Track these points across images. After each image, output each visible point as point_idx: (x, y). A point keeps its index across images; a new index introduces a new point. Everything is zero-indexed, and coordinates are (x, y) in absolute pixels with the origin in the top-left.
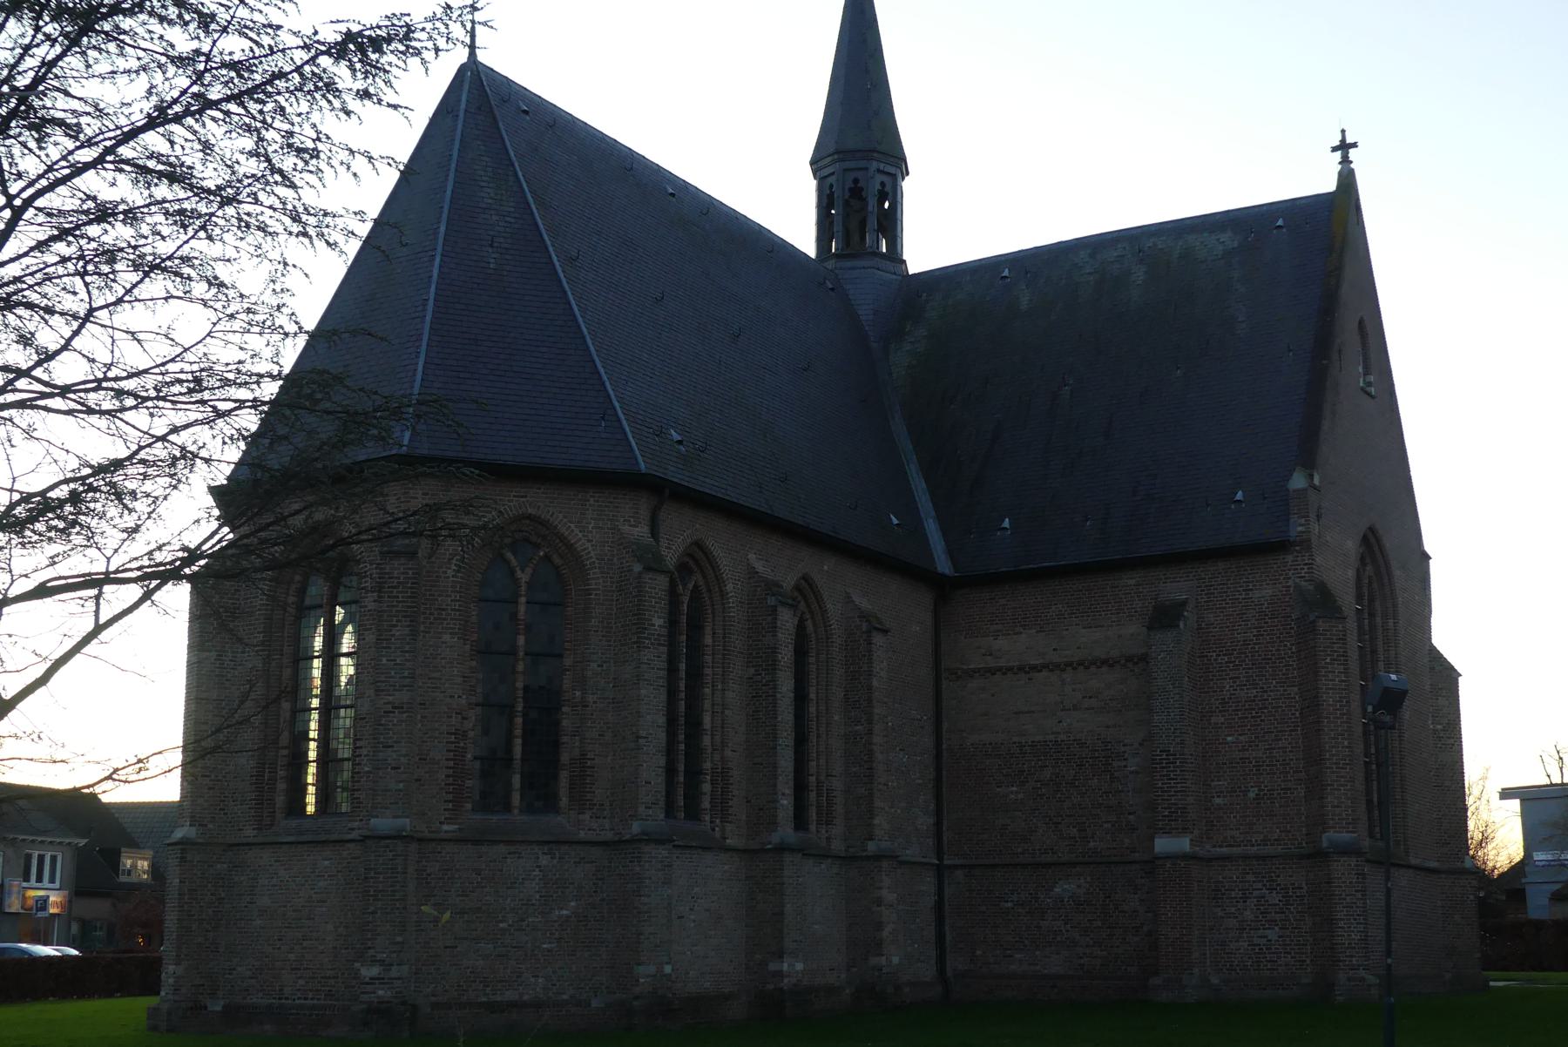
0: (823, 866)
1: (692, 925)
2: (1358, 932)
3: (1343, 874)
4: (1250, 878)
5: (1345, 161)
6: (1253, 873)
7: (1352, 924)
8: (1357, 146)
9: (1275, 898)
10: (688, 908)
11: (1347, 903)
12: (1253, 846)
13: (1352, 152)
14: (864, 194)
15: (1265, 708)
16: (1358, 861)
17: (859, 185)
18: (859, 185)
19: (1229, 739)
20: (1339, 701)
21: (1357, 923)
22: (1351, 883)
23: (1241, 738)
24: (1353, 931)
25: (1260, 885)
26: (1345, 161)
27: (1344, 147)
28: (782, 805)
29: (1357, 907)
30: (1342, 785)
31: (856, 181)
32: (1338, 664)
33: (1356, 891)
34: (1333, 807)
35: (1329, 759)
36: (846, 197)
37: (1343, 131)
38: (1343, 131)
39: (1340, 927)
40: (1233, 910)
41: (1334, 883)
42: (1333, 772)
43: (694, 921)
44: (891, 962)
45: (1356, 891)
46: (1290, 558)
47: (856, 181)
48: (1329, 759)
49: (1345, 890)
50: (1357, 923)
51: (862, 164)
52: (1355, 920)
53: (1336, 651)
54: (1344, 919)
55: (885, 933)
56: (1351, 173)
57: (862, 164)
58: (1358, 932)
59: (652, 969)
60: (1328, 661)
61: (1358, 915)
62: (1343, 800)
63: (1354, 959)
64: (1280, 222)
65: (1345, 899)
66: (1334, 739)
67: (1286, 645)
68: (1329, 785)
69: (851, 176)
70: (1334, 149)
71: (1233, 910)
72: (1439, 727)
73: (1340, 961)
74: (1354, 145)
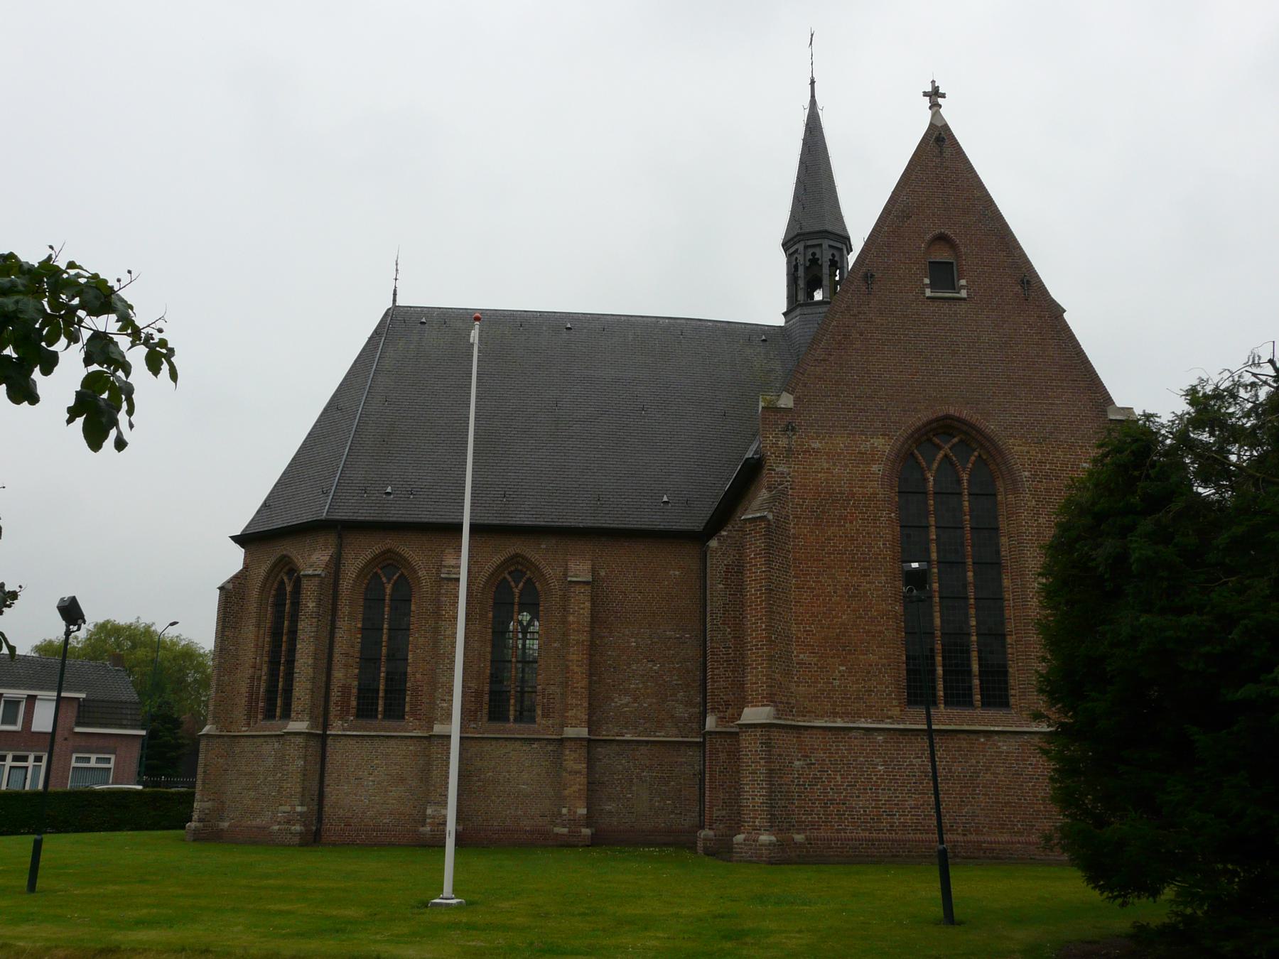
0: (535, 746)
1: (371, 783)
2: (761, 796)
3: (751, 744)
7: (756, 788)
10: (366, 773)
11: (752, 770)
16: (762, 731)
20: (758, 590)
21: (761, 788)
22: (756, 751)
24: (756, 795)
26: (935, 106)
27: (934, 95)
28: (442, 707)
29: (761, 773)
30: (759, 664)
32: (760, 558)
33: (760, 758)
34: (751, 684)
35: (749, 642)
39: (747, 792)
41: (743, 751)
42: (754, 653)
43: (373, 781)
44: (575, 812)
45: (760, 758)
48: (749, 642)
49: (751, 758)
50: (761, 788)
52: (758, 784)
53: (758, 547)
54: (749, 784)
55: (566, 792)
58: (761, 796)
59: (287, 808)
60: (752, 556)
61: (760, 781)
62: (760, 677)
63: (757, 820)
65: (751, 766)
66: (754, 623)
68: (749, 665)
73: (745, 822)
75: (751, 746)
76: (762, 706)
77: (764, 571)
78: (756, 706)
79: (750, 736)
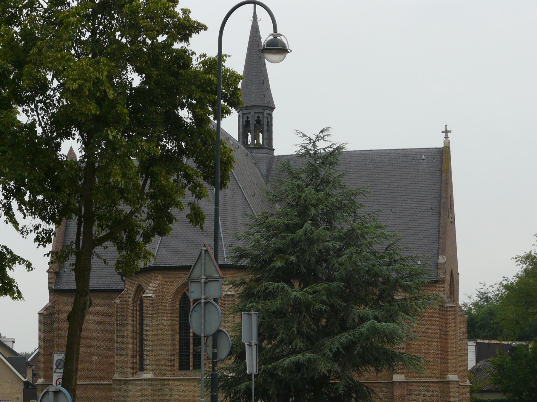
4: (421, 388)
5: (447, 137)
6: (422, 387)
8: (451, 132)
9: (429, 395)
12: (422, 378)
13: (449, 133)
14: (262, 122)
15: (428, 334)
17: (260, 119)
18: (260, 119)
19: (415, 343)
23: (420, 343)
25: (424, 391)
26: (447, 137)
31: (258, 117)
34: (450, 366)
36: (255, 123)
37: (446, 126)
38: (446, 126)
40: (415, 398)
46: (437, 285)
47: (258, 117)
51: (261, 111)
56: (449, 142)
57: (261, 111)
64: (423, 157)
67: (435, 314)
68: (449, 360)
69: (257, 115)
70: (443, 132)
71: (415, 398)
72: (461, 335)
74: (450, 132)
75: (453, 387)
76: (455, 374)
77: (454, 327)
78: (452, 374)
79: (453, 385)
